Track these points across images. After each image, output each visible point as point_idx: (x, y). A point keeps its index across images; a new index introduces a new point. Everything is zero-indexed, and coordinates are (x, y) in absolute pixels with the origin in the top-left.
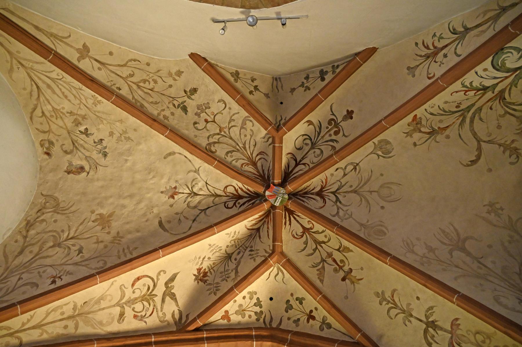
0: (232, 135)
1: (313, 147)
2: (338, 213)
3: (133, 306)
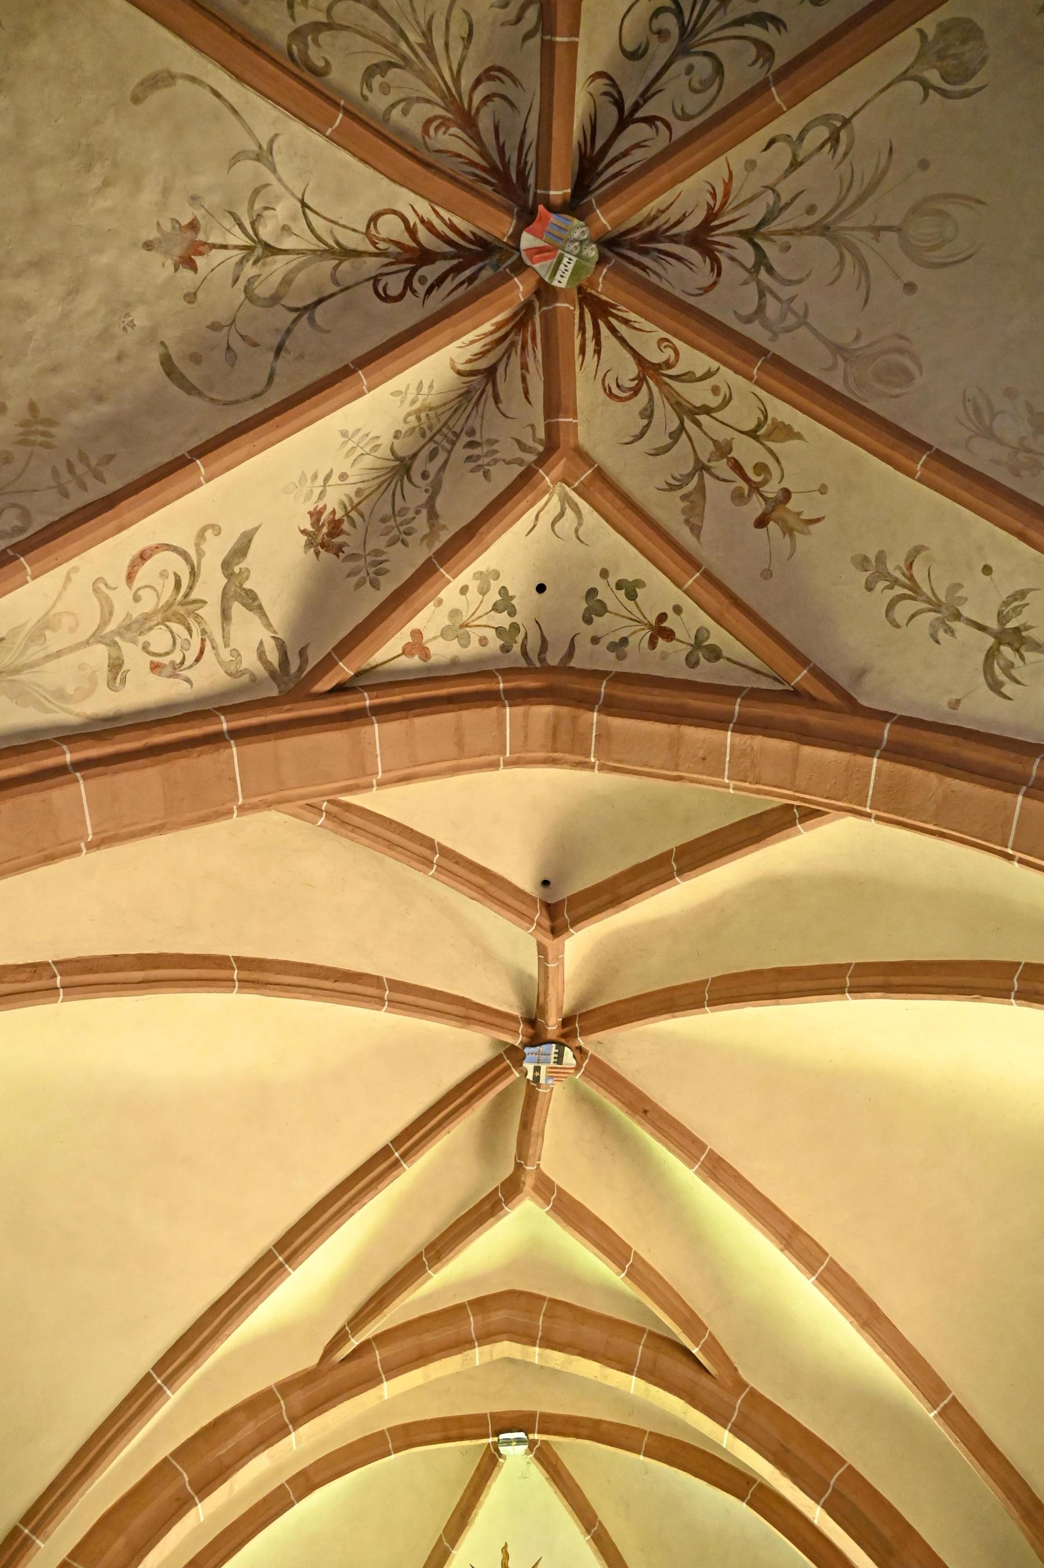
1: (683, 50)
2: (761, 308)
3: (142, 639)
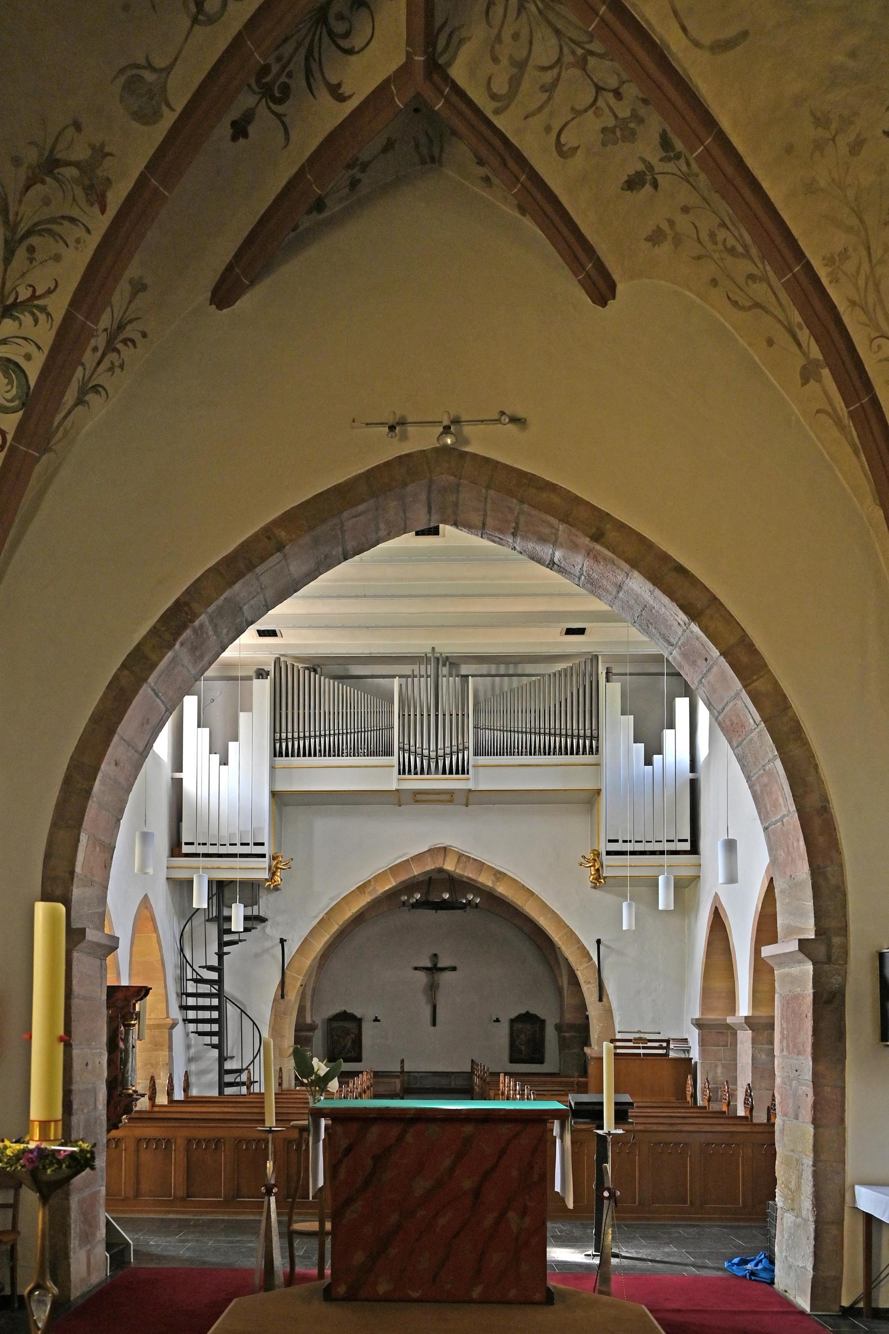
0: (553, 41)
